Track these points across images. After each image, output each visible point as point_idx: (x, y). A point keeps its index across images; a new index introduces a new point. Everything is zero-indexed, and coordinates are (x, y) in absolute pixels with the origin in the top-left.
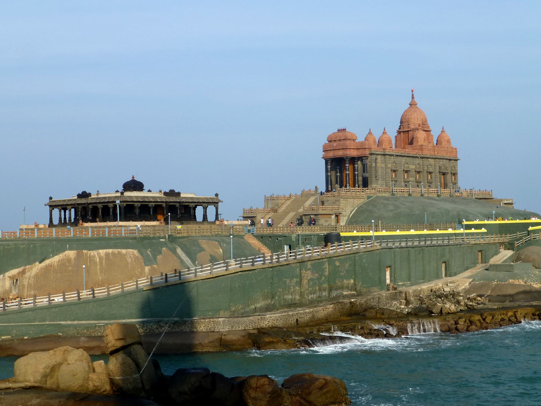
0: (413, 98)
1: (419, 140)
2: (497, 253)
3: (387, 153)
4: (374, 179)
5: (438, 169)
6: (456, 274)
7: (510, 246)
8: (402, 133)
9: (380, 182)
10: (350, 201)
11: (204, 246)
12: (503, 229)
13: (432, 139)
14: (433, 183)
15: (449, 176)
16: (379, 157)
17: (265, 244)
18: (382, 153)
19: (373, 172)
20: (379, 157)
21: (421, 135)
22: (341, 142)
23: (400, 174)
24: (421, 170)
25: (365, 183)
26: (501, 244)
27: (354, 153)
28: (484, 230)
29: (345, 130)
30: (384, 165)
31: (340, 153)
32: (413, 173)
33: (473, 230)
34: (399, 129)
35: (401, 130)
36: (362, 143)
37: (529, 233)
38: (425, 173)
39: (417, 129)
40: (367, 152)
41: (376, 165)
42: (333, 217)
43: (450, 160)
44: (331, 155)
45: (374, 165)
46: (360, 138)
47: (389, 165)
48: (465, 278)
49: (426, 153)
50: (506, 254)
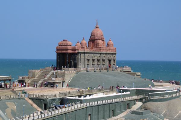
0: (97, 24)
1: (99, 45)
2: (135, 104)
4: (79, 64)
5: (107, 58)
6: (117, 115)
7: (141, 100)
9: (82, 65)
10: (69, 75)
11: (8, 105)
12: (138, 92)
13: (105, 44)
14: (105, 65)
15: (112, 61)
17: (34, 102)
18: (83, 52)
19: (79, 60)
20: (82, 54)
21: (100, 42)
22: (65, 46)
23: (91, 61)
24: (100, 59)
25: (75, 66)
26: (137, 100)
28: (129, 93)
29: (66, 40)
30: (84, 57)
31: (65, 51)
32: (96, 60)
33: (125, 93)
36: (75, 48)
37: (149, 95)
38: (102, 60)
39: (98, 39)
40: (77, 51)
42: (62, 84)
44: (60, 51)
45: (79, 57)
46: (73, 45)
47: (86, 57)
48: (122, 117)
50: (139, 104)
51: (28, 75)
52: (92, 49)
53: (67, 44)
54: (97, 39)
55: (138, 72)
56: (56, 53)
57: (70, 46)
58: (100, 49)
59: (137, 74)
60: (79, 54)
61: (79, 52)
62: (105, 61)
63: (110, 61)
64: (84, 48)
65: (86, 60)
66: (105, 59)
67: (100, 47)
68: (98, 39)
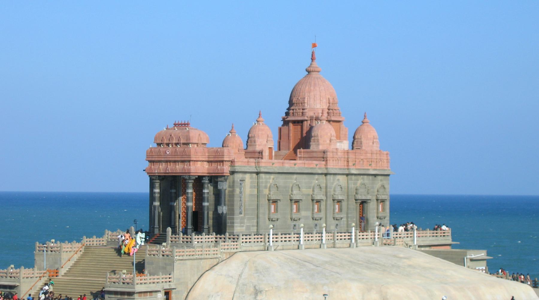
0: (313, 59)
1: (321, 141)
3: (263, 170)
8: (291, 125)
16: (247, 176)
24: (324, 198)
27: (200, 168)
29: (186, 125)
34: (287, 114)
35: (290, 118)
38: (330, 201)
41: (241, 193)
43: (375, 175)
44: (161, 169)
49: (333, 166)
51: (30, 264)
52: (293, 157)
53: (188, 138)
54: (311, 119)
55: (477, 247)
56: (145, 173)
57: (200, 149)
58: (323, 156)
59: (473, 257)
60: (238, 177)
61: (237, 169)
62: (344, 204)
63: (363, 203)
64: (261, 152)
65: (264, 202)
66: (340, 198)
67: (321, 148)
68: (317, 119)
